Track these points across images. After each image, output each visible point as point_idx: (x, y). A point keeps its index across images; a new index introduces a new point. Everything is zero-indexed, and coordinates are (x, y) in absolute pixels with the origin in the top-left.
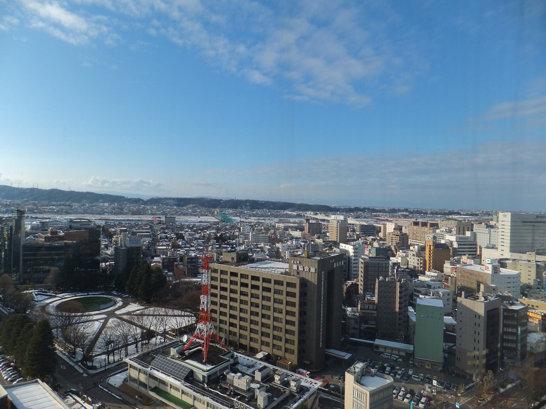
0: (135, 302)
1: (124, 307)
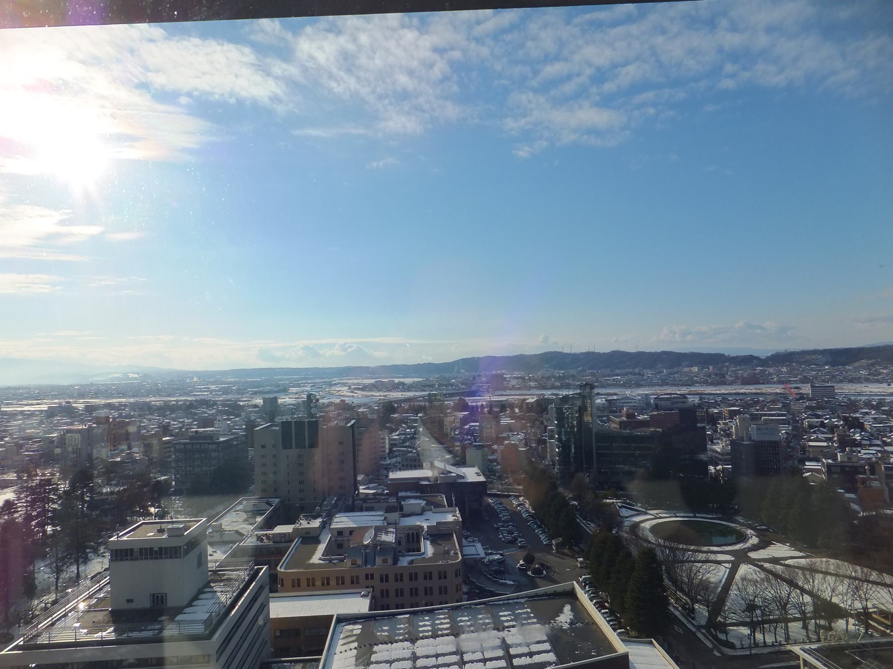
0: (783, 542)
1: (763, 548)
